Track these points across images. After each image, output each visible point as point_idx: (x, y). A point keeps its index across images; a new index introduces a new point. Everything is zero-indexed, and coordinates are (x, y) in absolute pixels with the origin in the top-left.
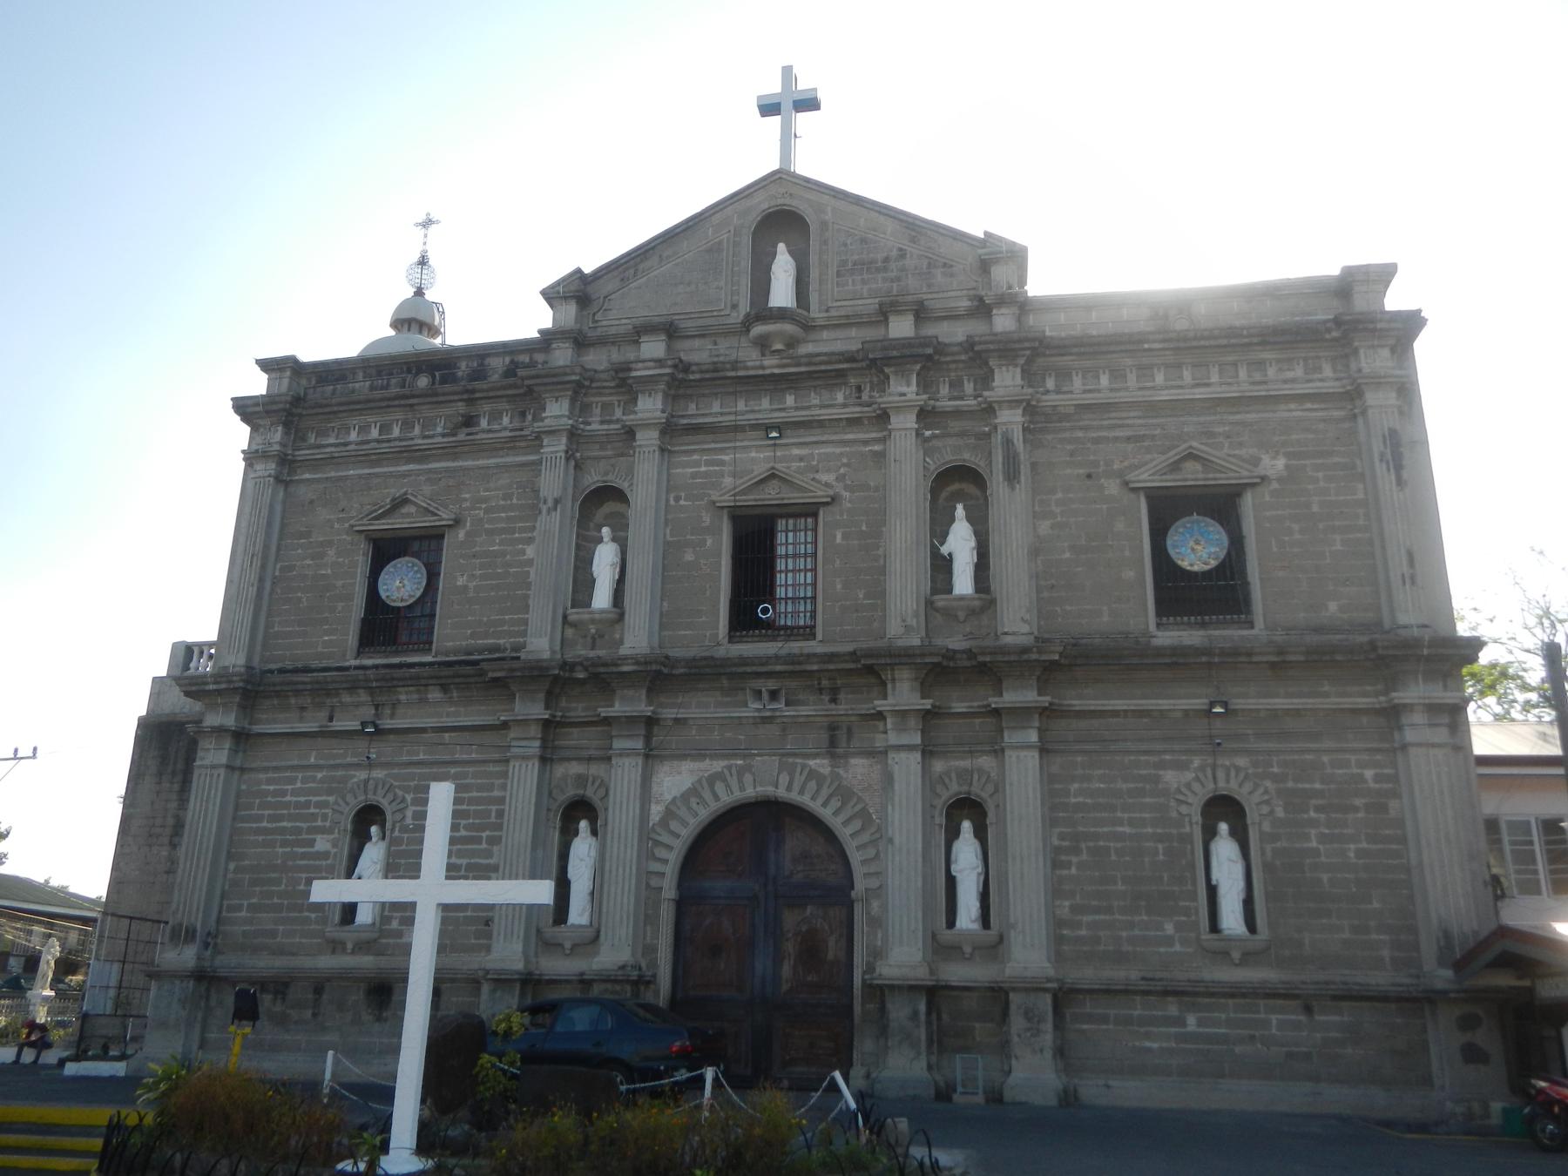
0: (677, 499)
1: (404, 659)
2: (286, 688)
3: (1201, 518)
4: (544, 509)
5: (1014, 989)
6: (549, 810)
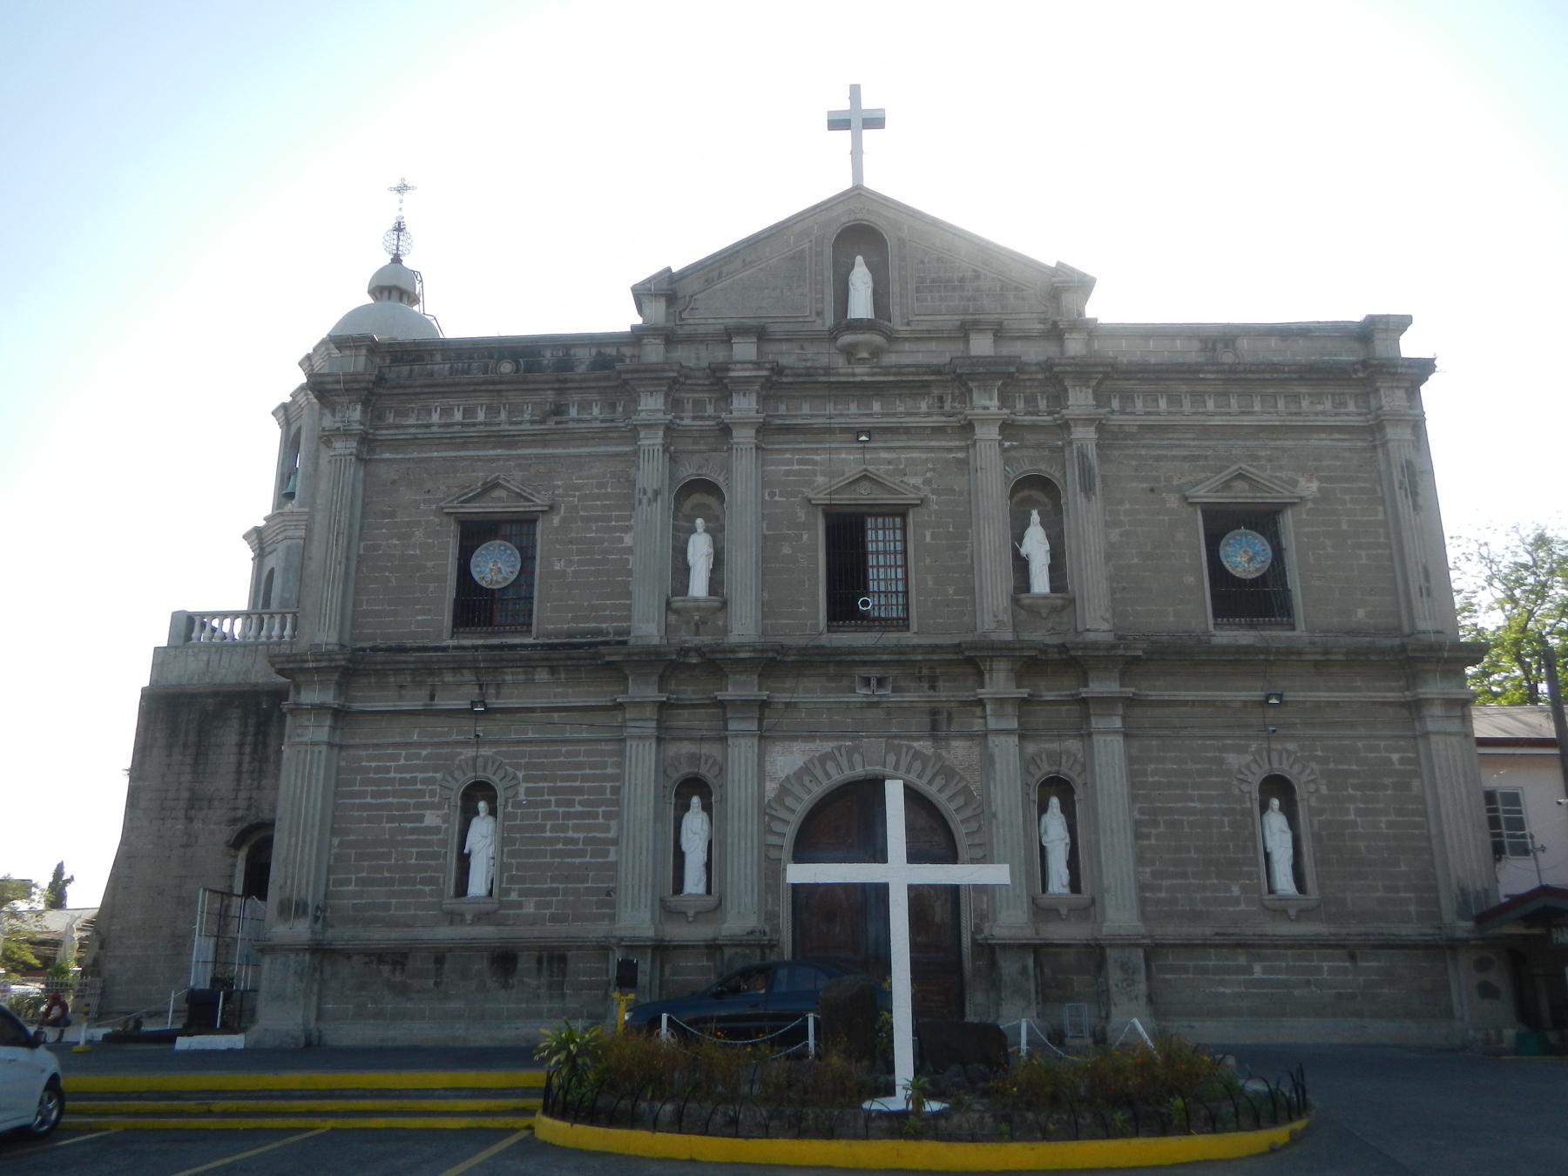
0: (772, 495)
1: (504, 640)
2: (387, 667)
3: (1248, 531)
4: (645, 501)
5: (1111, 946)
6: (664, 787)
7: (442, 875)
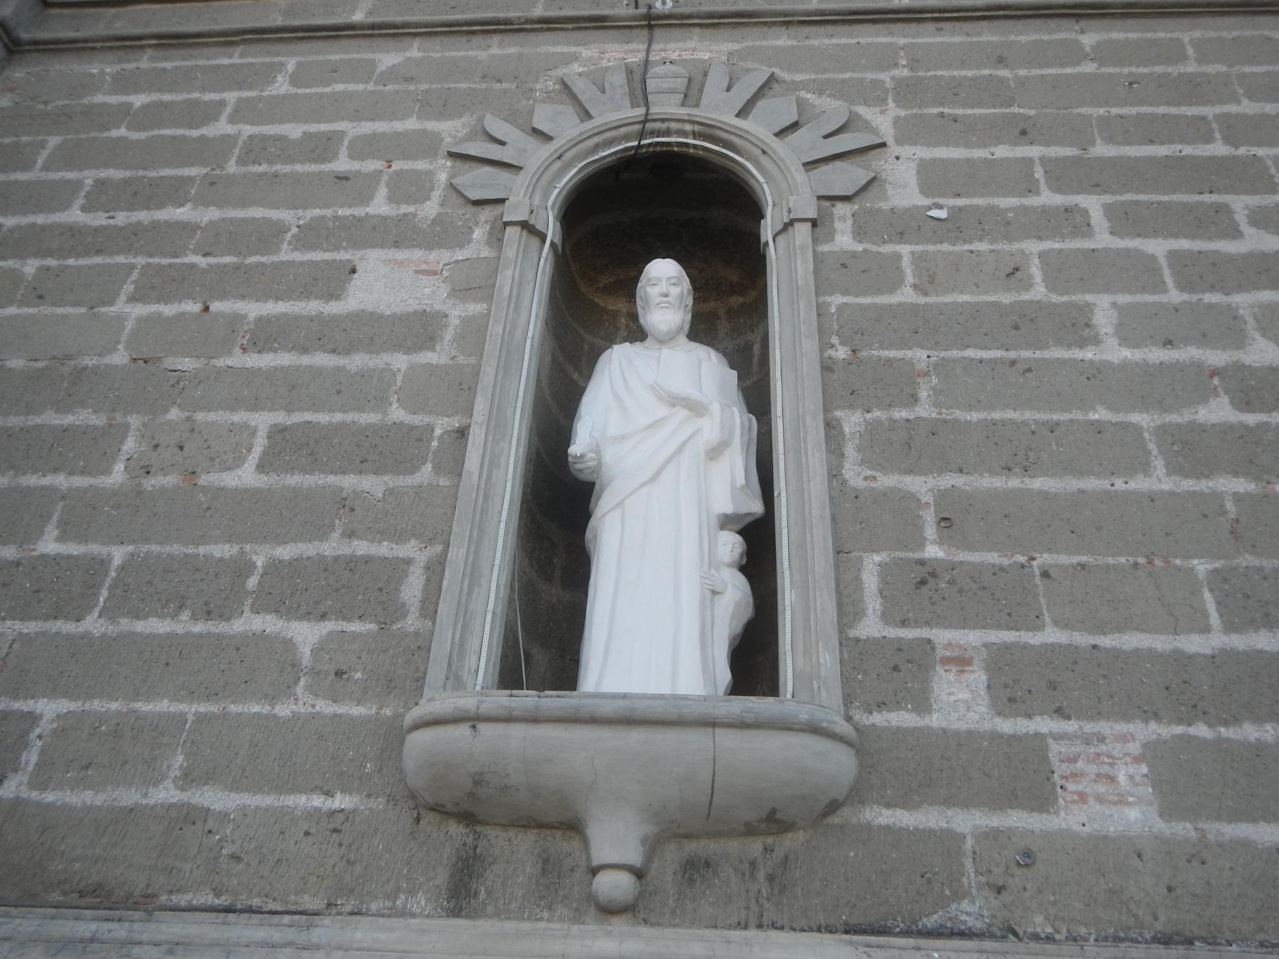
7: (409, 549)
